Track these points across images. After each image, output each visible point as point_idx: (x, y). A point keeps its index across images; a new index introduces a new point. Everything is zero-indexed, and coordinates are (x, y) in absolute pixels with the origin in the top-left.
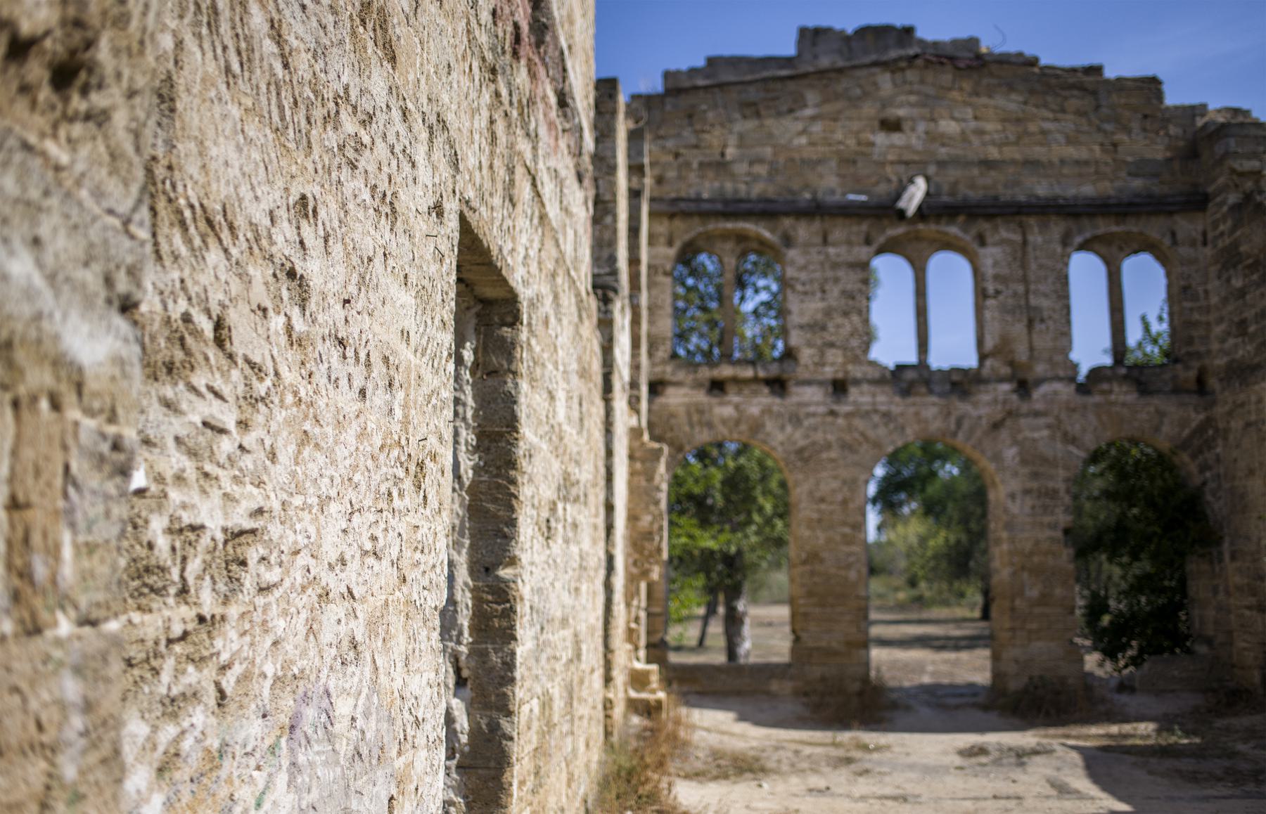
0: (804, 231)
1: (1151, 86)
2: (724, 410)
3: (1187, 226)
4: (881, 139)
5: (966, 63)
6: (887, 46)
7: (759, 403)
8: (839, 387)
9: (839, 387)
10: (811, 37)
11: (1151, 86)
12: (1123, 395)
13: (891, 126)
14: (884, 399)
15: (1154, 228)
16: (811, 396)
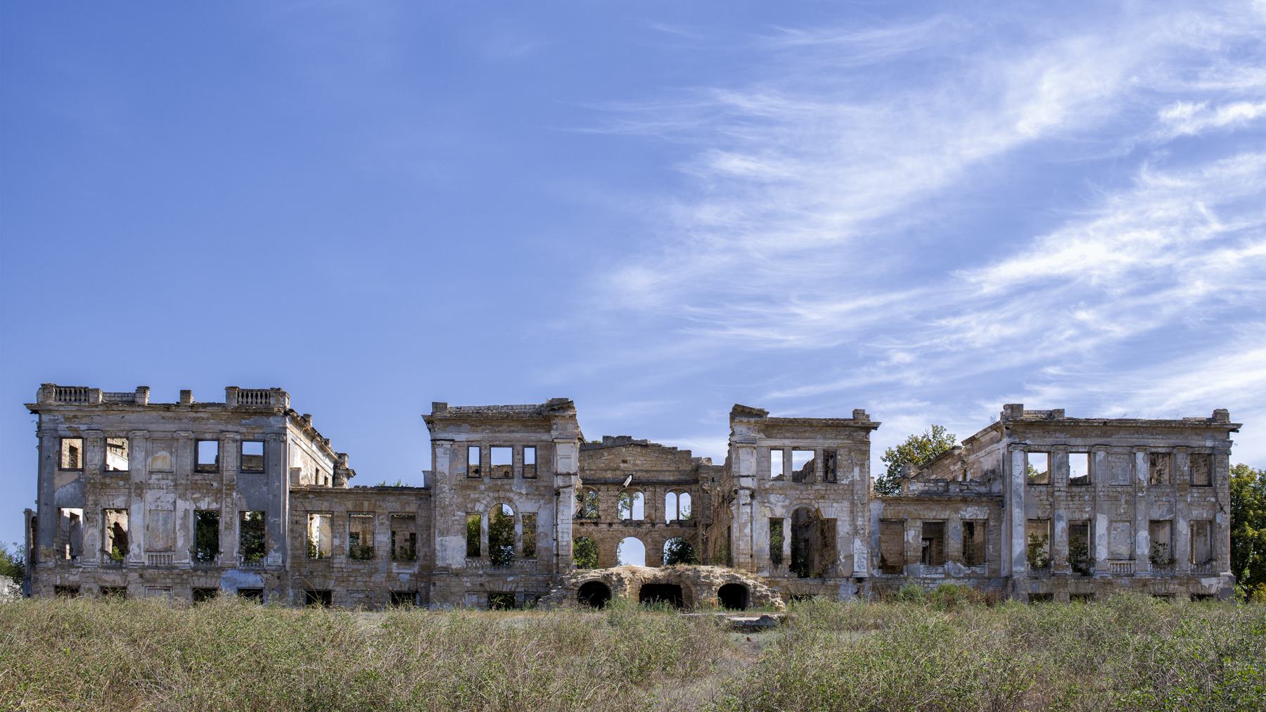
0: (602, 487)
1: (689, 452)
2: (583, 529)
3: (693, 487)
4: (622, 465)
5: (644, 445)
6: (625, 441)
7: (593, 527)
8: (610, 525)
9: (610, 525)
10: (605, 438)
11: (689, 452)
12: (676, 527)
13: (625, 462)
14: (621, 527)
15: (686, 487)
16: (604, 527)
